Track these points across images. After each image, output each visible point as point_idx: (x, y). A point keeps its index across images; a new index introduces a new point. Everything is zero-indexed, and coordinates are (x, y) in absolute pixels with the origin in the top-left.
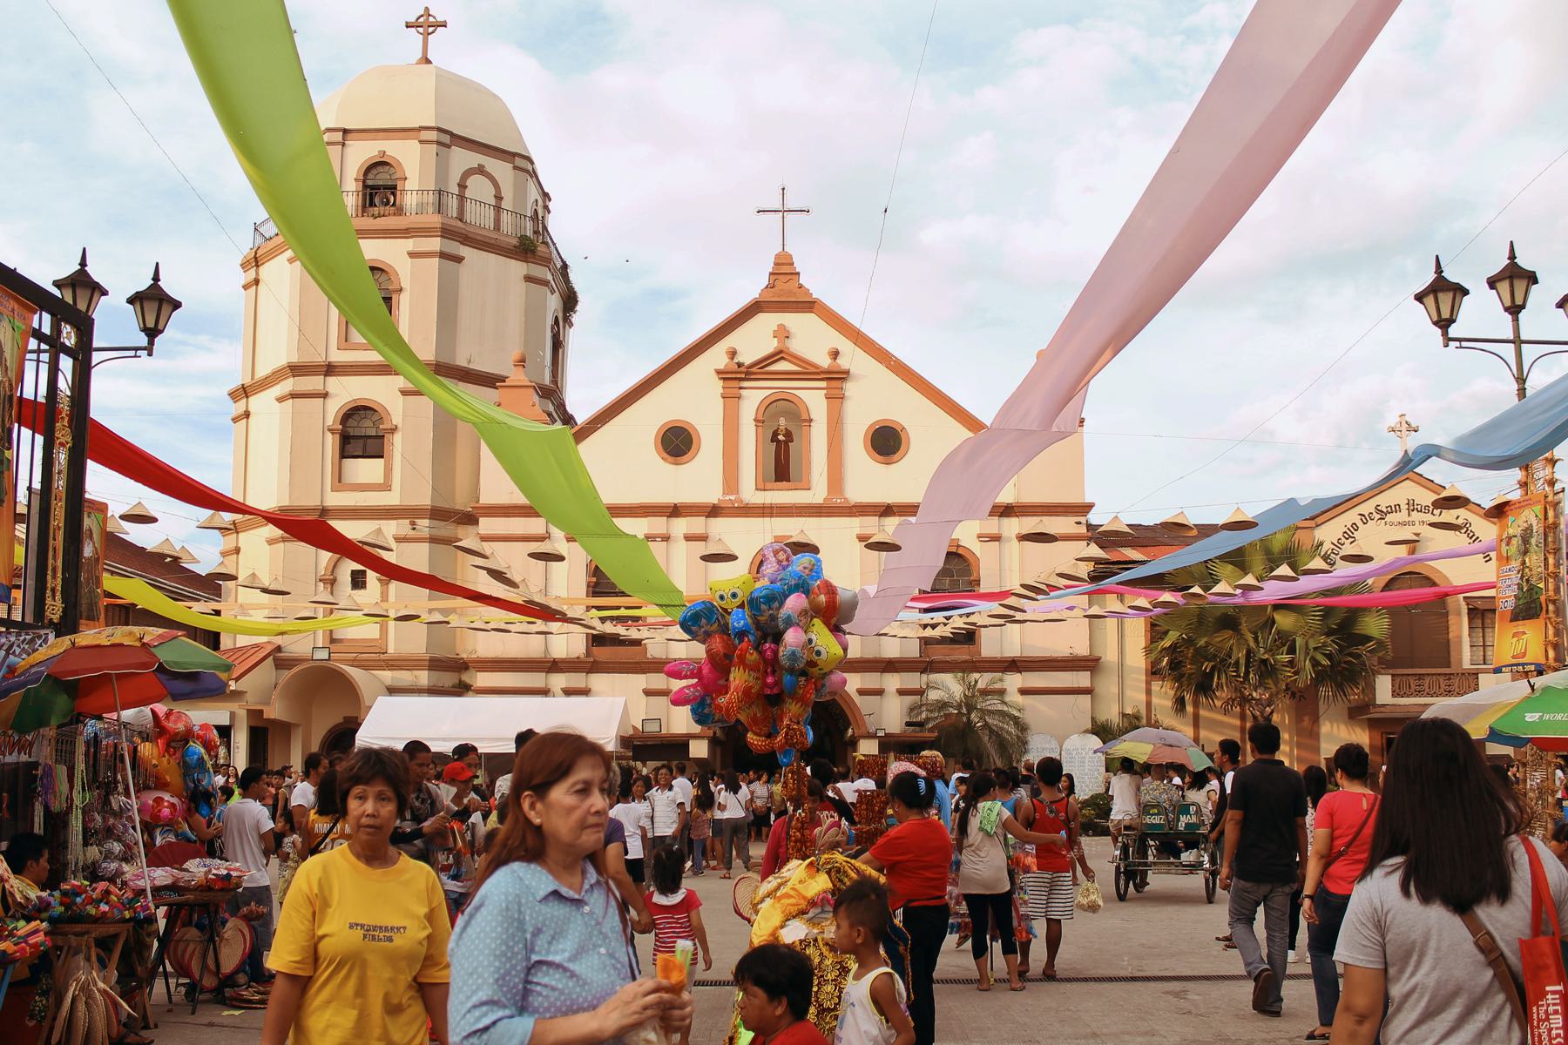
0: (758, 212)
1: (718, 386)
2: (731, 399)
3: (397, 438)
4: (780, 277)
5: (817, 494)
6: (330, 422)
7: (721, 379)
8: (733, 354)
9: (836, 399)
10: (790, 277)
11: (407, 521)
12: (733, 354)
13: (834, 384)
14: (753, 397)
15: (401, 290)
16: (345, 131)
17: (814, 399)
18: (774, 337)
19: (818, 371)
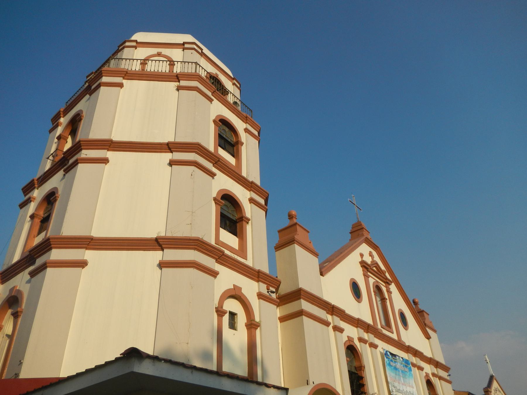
0: (350, 201)
1: (361, 269)
2: (366, 277)
3: (249, 228)
4: (366, 231)
5: (394, 336)
6: (214, 195)
7: (361, 266)
8: (362, 255)
9: (389, 292)
10: (368, 233)
11: (265, 286)
12: (362, 255)
13: (387, 285)
14: (371, 281)
15: (242, 144)
16: (202, 52)
17: (384, 289)
18: (370, 256)
19: (385, 277)
